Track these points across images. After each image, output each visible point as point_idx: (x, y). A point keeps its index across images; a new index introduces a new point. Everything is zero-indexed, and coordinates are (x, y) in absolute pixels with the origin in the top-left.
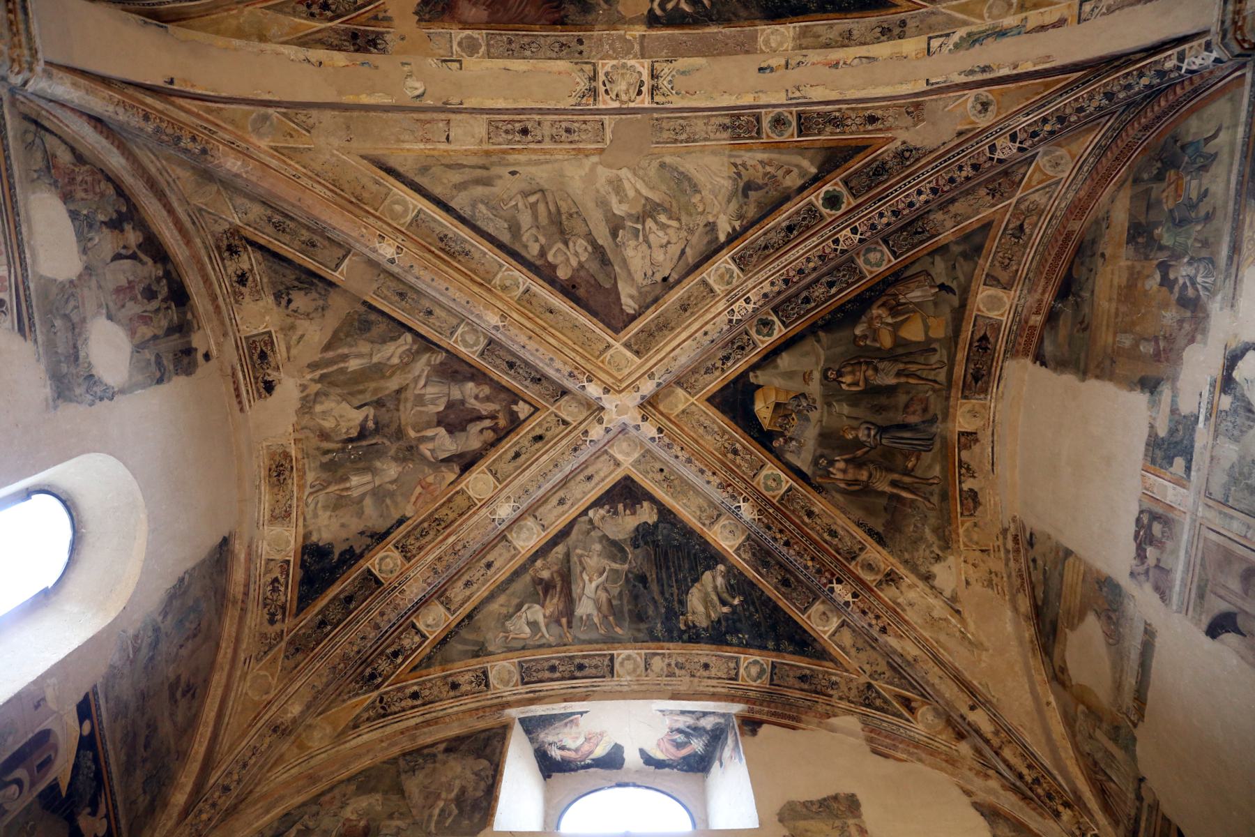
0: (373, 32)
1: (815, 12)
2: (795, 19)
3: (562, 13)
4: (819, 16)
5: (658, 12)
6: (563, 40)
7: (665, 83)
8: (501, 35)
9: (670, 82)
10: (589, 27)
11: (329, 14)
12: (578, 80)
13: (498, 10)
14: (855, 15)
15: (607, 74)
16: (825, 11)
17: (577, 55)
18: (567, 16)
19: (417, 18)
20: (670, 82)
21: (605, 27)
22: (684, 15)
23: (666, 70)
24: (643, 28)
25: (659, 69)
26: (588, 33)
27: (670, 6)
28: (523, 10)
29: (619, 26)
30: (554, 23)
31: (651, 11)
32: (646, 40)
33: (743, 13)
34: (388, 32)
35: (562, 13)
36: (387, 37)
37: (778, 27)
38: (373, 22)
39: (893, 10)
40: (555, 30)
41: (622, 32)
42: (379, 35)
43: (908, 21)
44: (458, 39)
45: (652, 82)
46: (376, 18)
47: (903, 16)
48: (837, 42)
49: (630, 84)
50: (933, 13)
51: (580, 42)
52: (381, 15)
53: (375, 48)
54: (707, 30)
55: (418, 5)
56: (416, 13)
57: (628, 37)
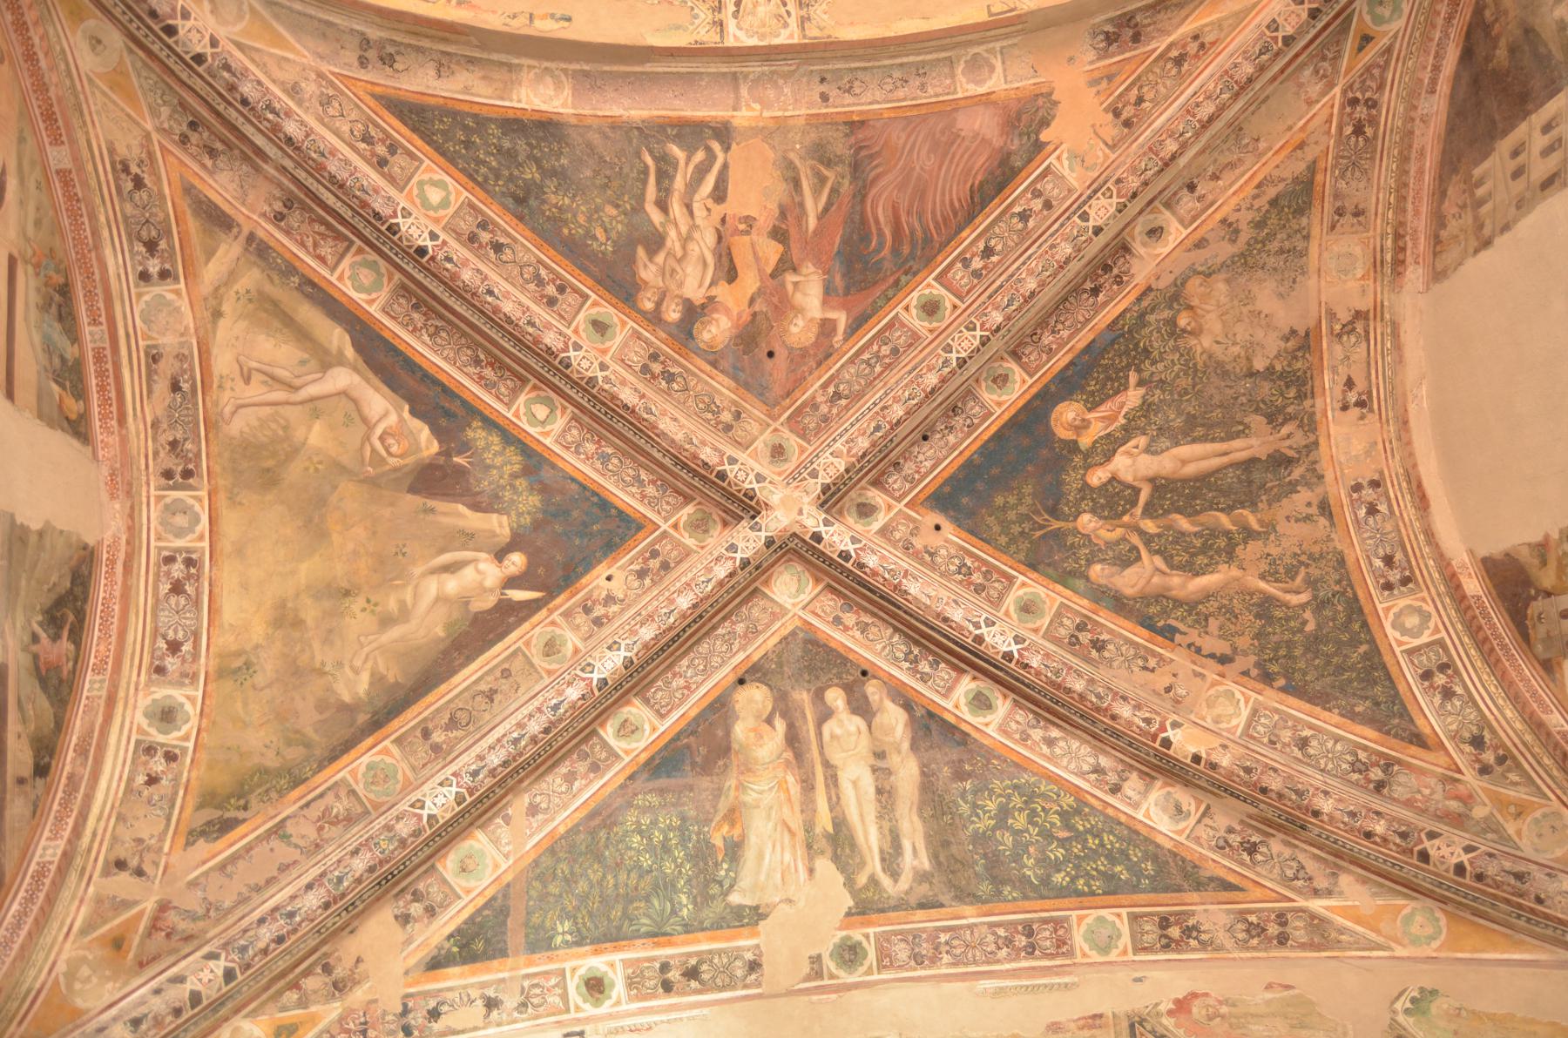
0: (1113, 55)
1: (490, 120)
2: (519, 114)
3: (852, 140)
4: (484, 112)
5: (716, 146)
6: (848, 99)
7: (703, 16)
8: (937, 95)
9: (696, 17)
10: (814, 121)
11: (1174, 53)
12: (825, 17)
13: (943, 133)
14: (432, 101)
15: (786, 25)
16: (475, 116)
17: (828, 77)
18: (846, 135)
19: (1054, 97)
20: (696, 17)
21: (791, 122)
22: (678, 139)
23: (703, 32)
24: (736, 123)
25: (712, 33)
26: (813, 111)
27: (700, 156)
28: (908, 137)
29: (771, 124)
30: (863, 123)
31: (727, 149)
32: (731, 102)
33: (595, 138)
34: (1092, 62)
35: (852, 140)
36: (1092, 55)
37: (544, 107)
38: (1114, 69)
39: (378, 90)
40: (861, 113)
41: (766, 114)
42: (1104, 54)
43: (356, 64)
44: (995, 77)
45: (722, 16)
46: (1110, 78)
47: (362, 75)
48: (458, 63)
49: (754, 14)
50: (322, 58)
51: (824, 98)
52: (1104, 84)
53: (1107, 33)
54: (645, 114)
55: (1054, 117)
56: (1056, 103)
57: (757, 106)
